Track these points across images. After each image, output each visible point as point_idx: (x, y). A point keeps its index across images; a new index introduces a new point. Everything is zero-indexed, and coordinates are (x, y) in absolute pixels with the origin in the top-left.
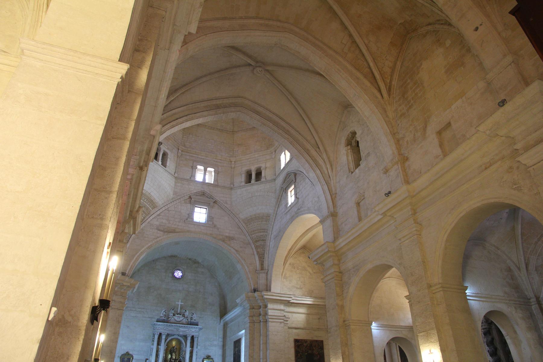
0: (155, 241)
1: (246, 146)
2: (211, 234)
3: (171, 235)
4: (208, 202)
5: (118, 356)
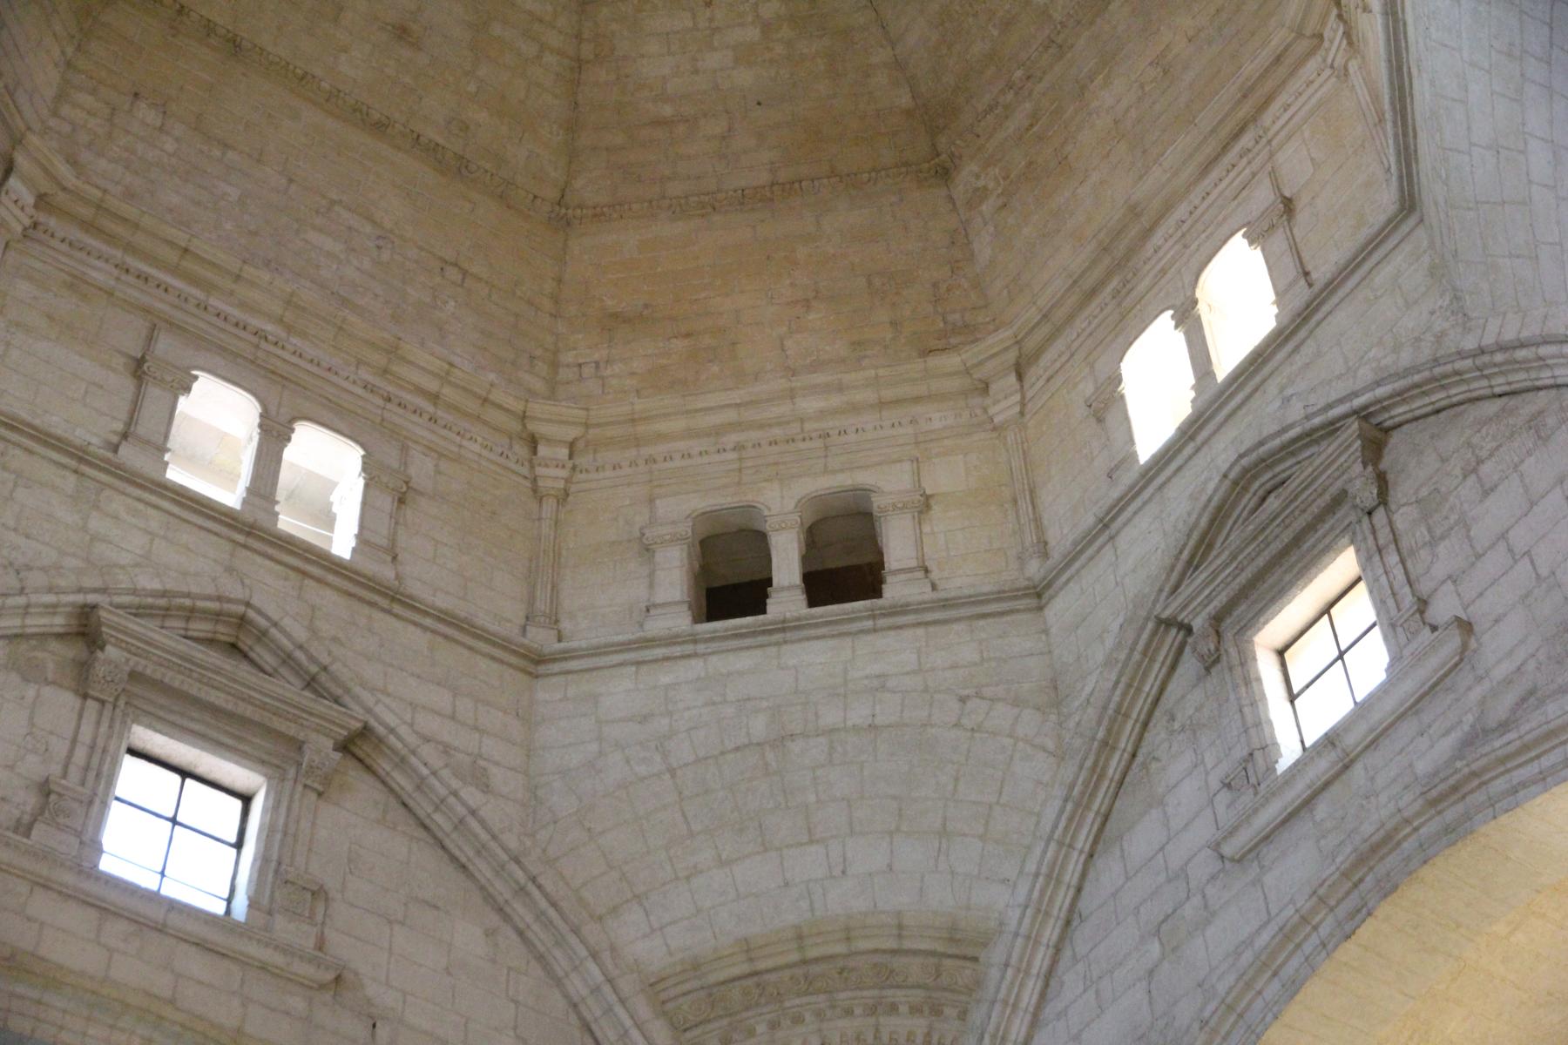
1: (688, 335)
4: (292, 730)
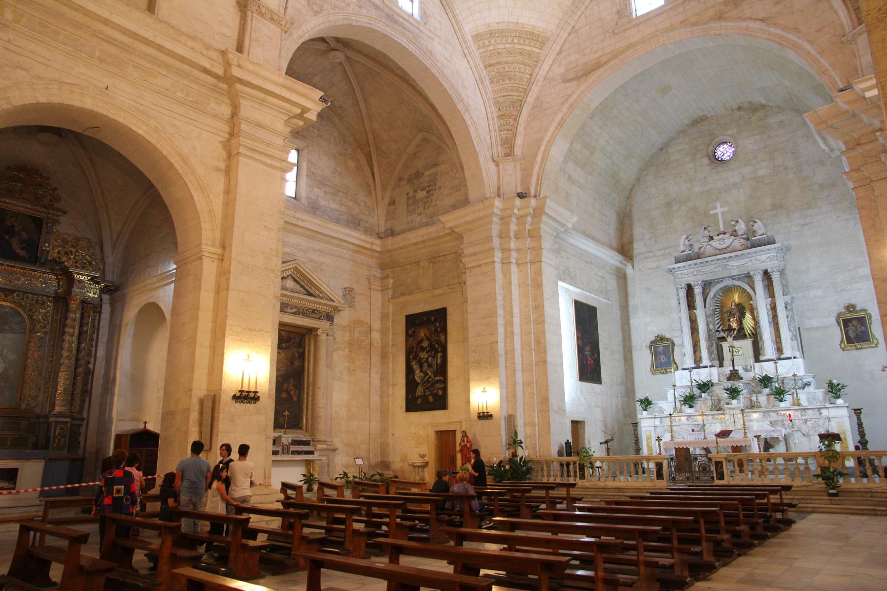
0: (567, 106)
2: (682, 22)
3: (594, 77)
5: (646, 346)
